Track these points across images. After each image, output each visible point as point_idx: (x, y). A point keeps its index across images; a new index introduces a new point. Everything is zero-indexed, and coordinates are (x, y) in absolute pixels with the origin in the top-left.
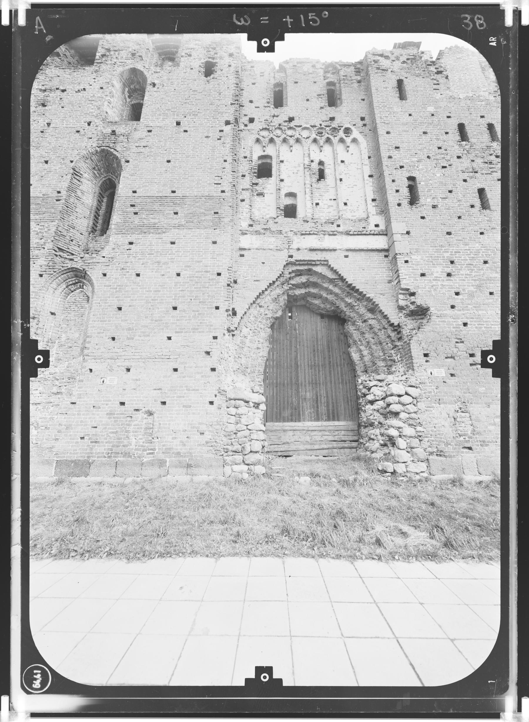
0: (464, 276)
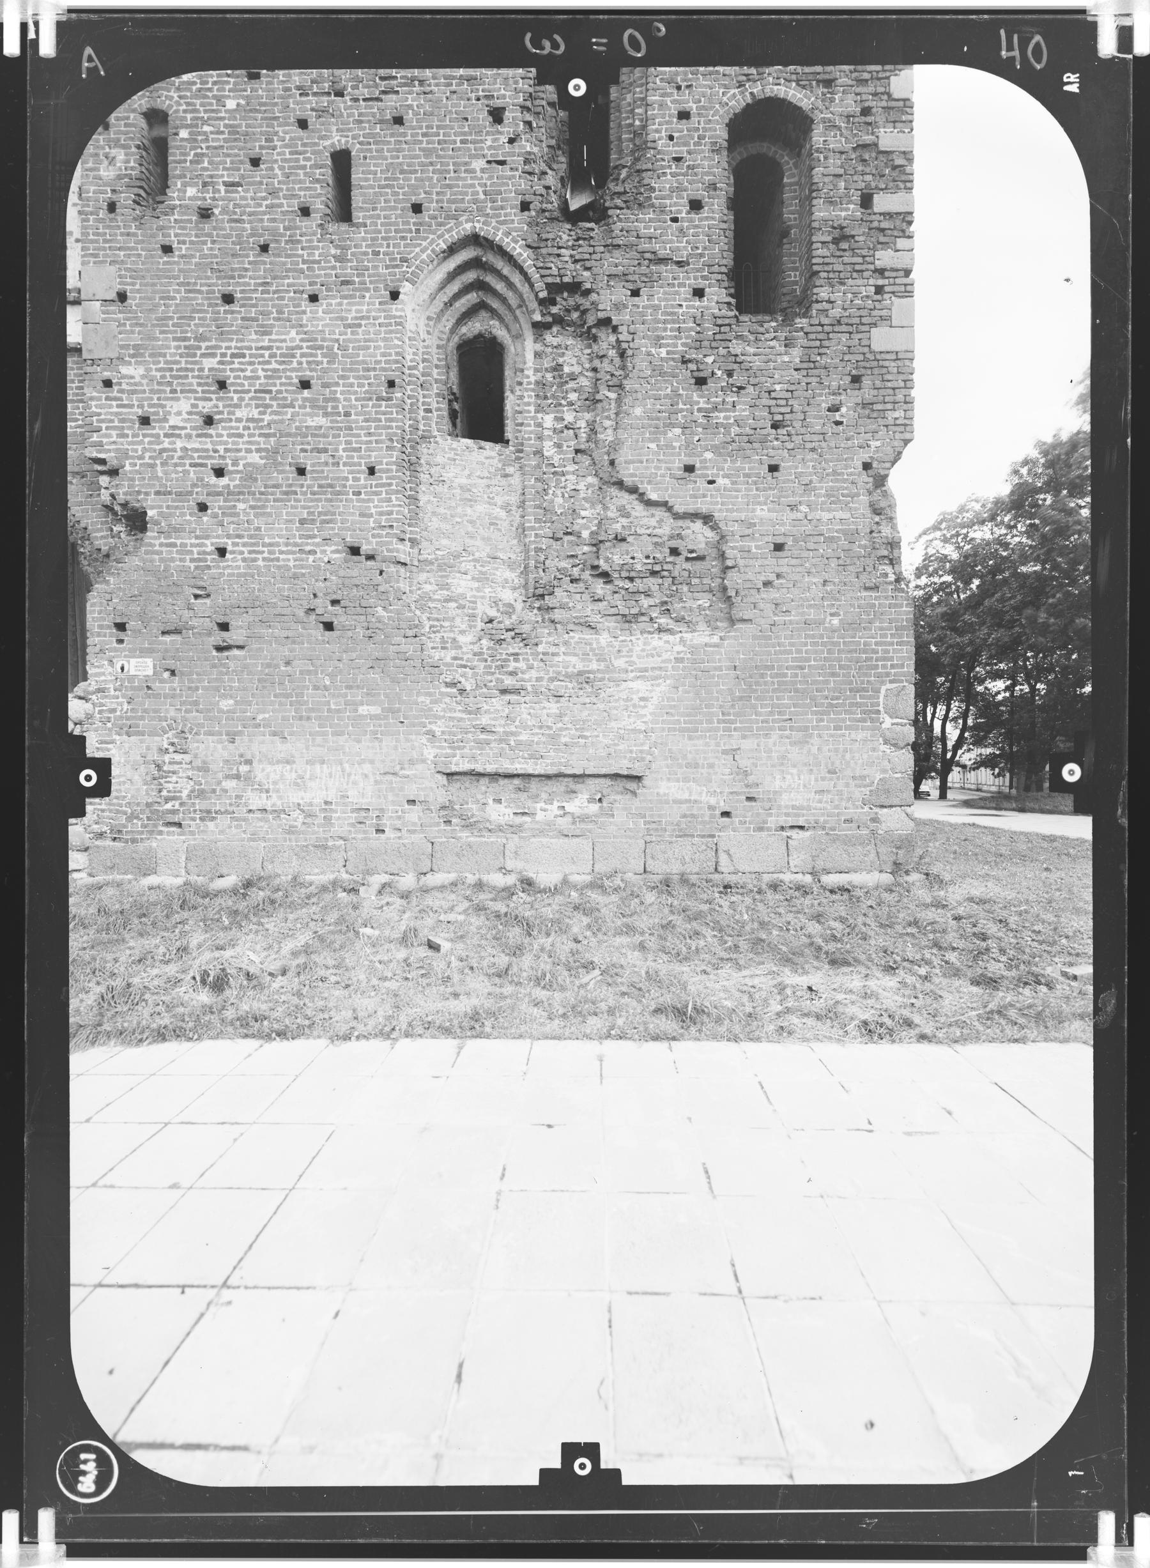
0: (241, 425)
